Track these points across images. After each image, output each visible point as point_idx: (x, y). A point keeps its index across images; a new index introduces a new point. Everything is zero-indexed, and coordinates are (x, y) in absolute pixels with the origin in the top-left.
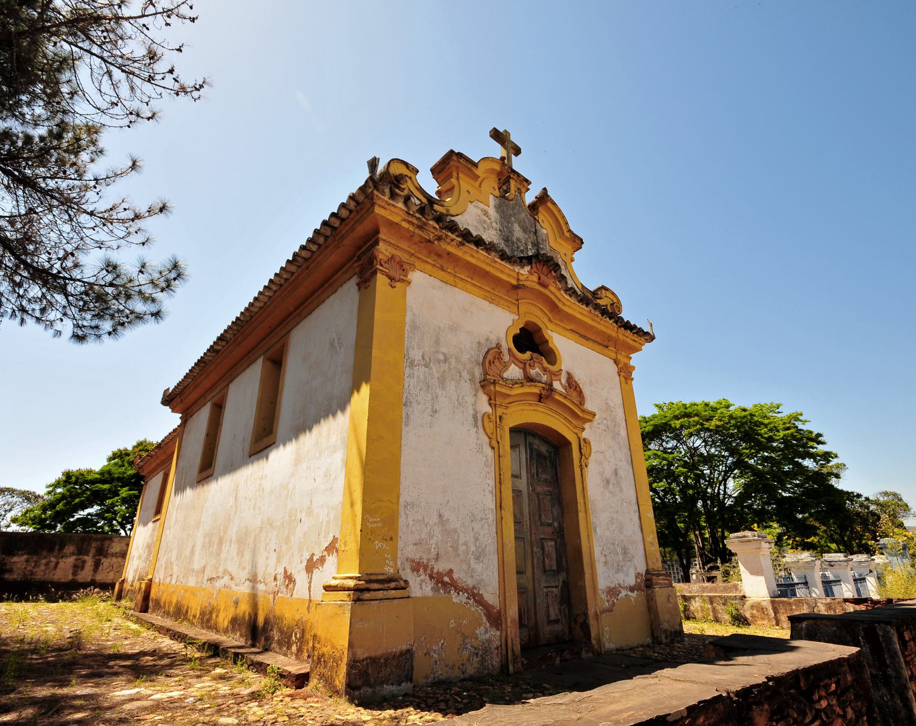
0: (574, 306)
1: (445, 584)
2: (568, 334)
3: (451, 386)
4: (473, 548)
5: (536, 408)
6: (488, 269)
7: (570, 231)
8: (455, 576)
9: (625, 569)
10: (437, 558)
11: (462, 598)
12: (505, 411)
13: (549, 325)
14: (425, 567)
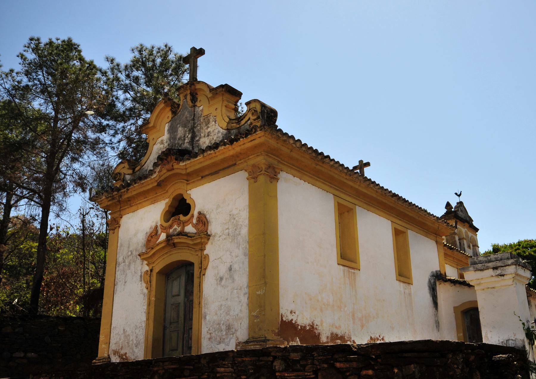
3: (132, 266)
4: (135, 342)
5: (171, 253)
8: (127, 355)
9: (226, 341)
10: (121, 349)
12: (153, 265)
13: (189, 187)
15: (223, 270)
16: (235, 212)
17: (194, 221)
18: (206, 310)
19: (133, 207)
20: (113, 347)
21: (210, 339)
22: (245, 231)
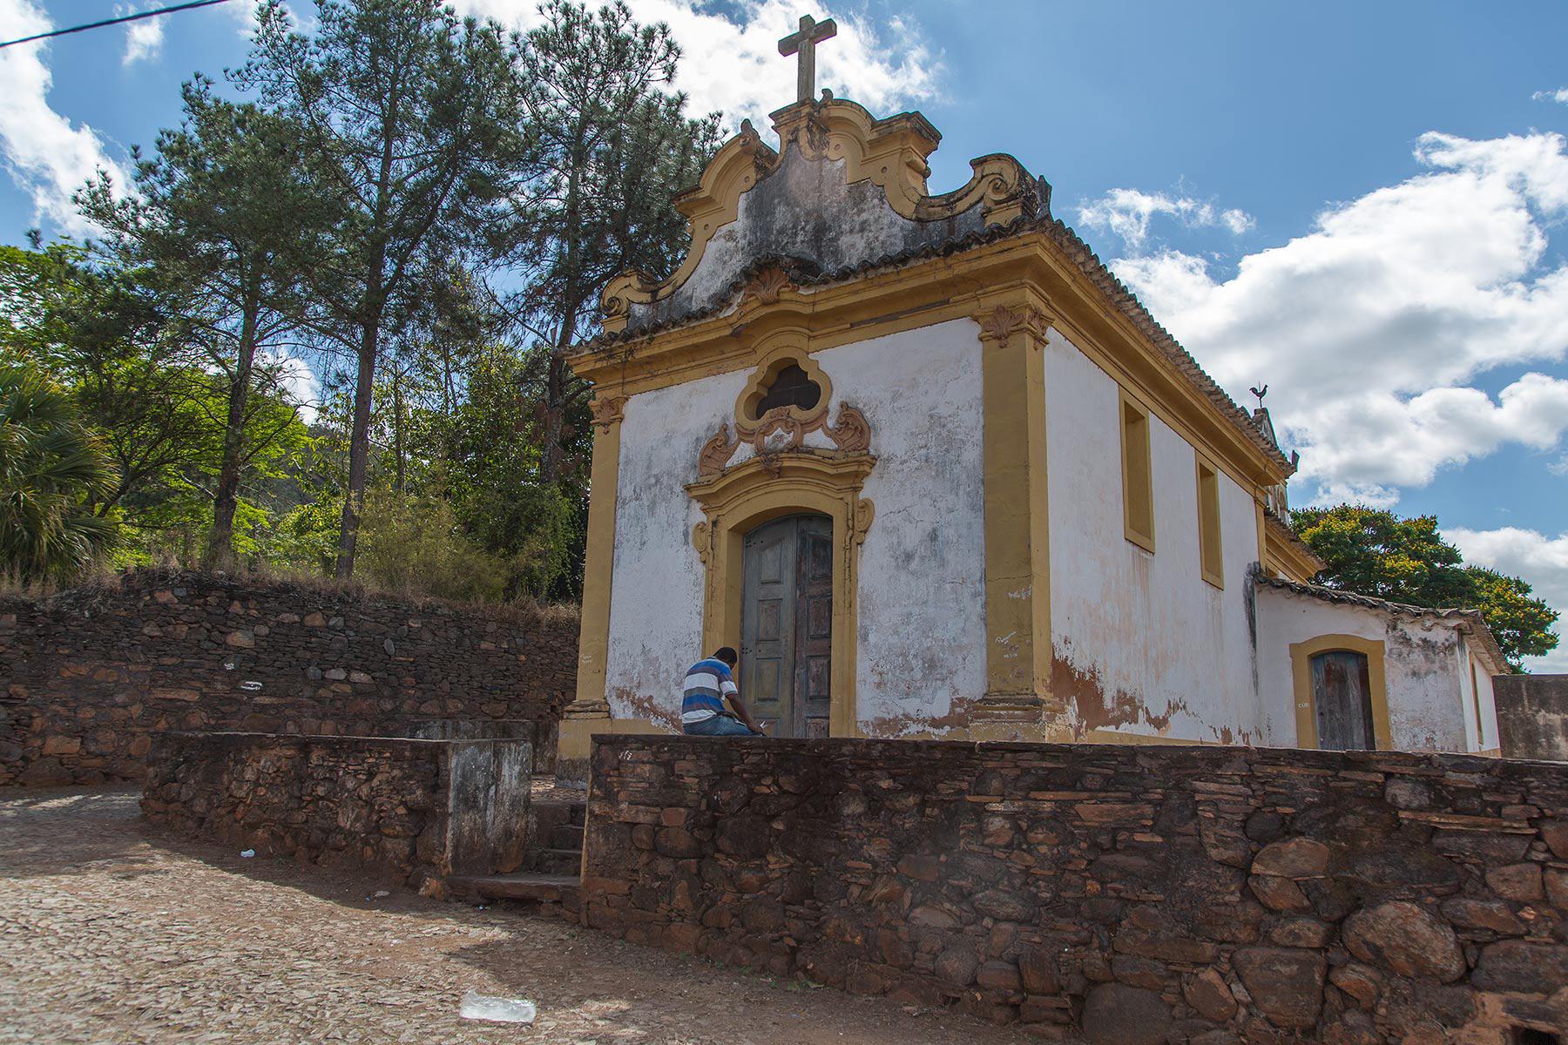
0: (832, 294)
1: (644, 709)
2: (852, 335)
3: (661, 509)
4: (674, 675)
6: (690, 342)
7: (875, 124)
8: (655, 702)
9: (924, 692)
10: (639, 686)
11: (661, 721)
13: (813, 344)
14: (628, 694)
15: (913, 537)
16: (943, 410)
17: (831, 422)
18: (868, 622)
19: (658, 380)
20: (614, 680)
21: (879, 685)
22: (972, 455)
